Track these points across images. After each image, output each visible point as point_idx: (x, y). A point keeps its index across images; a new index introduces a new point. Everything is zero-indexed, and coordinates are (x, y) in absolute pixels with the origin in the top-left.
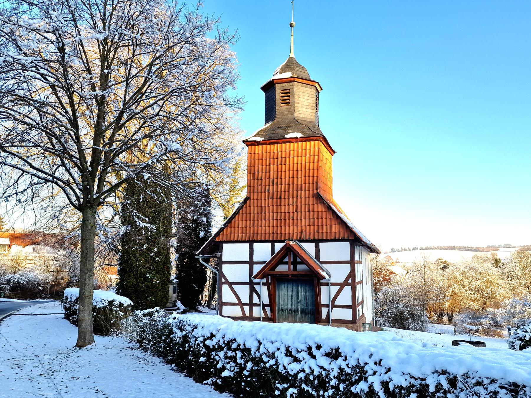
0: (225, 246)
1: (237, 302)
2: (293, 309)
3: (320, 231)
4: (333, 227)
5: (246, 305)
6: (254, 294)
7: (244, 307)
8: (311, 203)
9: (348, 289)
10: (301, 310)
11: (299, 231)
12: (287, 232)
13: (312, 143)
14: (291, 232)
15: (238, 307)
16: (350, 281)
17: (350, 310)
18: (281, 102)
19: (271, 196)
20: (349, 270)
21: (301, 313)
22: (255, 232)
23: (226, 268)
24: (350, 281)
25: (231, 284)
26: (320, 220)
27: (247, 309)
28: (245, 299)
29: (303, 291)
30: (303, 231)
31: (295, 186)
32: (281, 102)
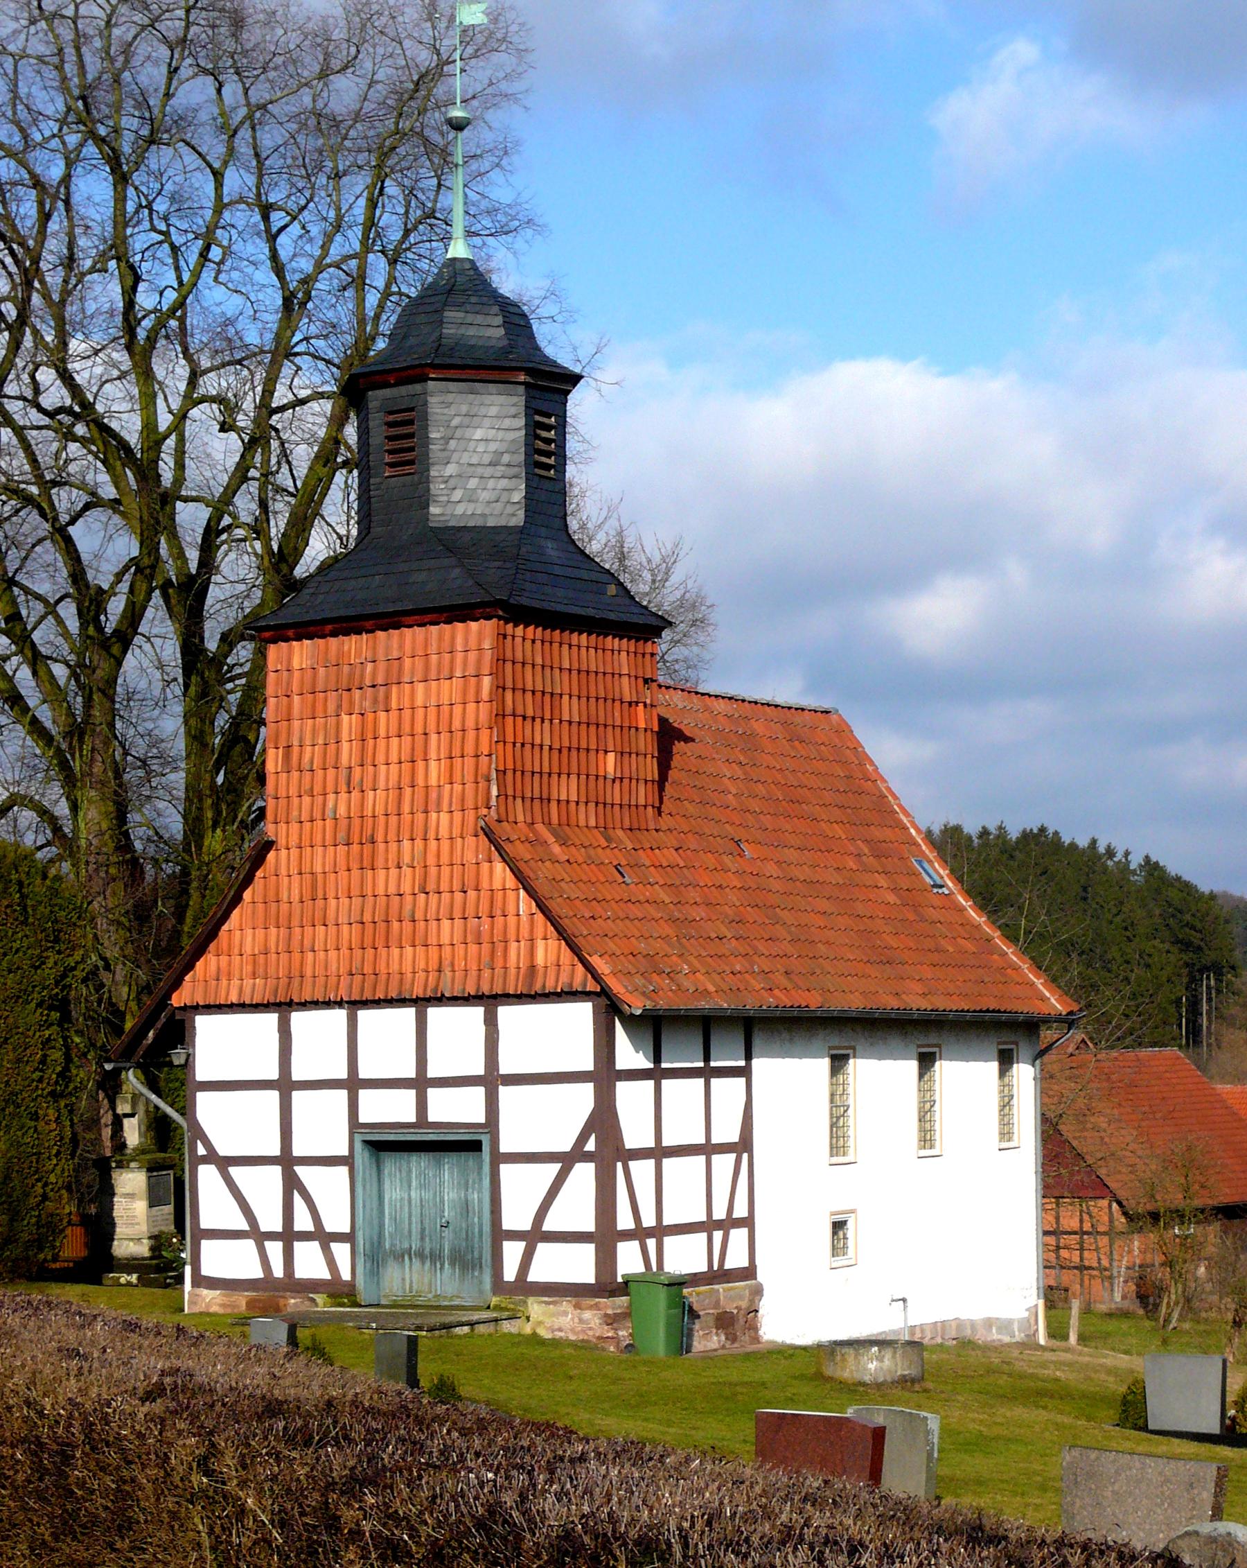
0: (204, 1024)
1: (244, 1225)
2: (427, 1251)
3: (499, 963)
4: (540, 945)
5: (272, 1236)
6: (297, 1197)
7: (268, 1244)
8: (470, 857)
9: (584, 1174)
10: (451, 1250)
11: (433, 965)
12: (395, 967)
13: (474, 625)
14: (407, 968)
15: (250, 1244)
16: (590, 1146)
17: (589, 1250)
18: (388, 459)
19: (341, 836)
20: (590, 1105)
21: (452, 1264)
22: (295, 973)
23: (208, 1108)
24: (590, 1146)
25: (224, 1163)
26: (499, 920)
27: (275, 1249)
28: (271, 1220)
29: (459, 1183)
30: (446, 963)
31: (419, 792)
32: (388, 459)
